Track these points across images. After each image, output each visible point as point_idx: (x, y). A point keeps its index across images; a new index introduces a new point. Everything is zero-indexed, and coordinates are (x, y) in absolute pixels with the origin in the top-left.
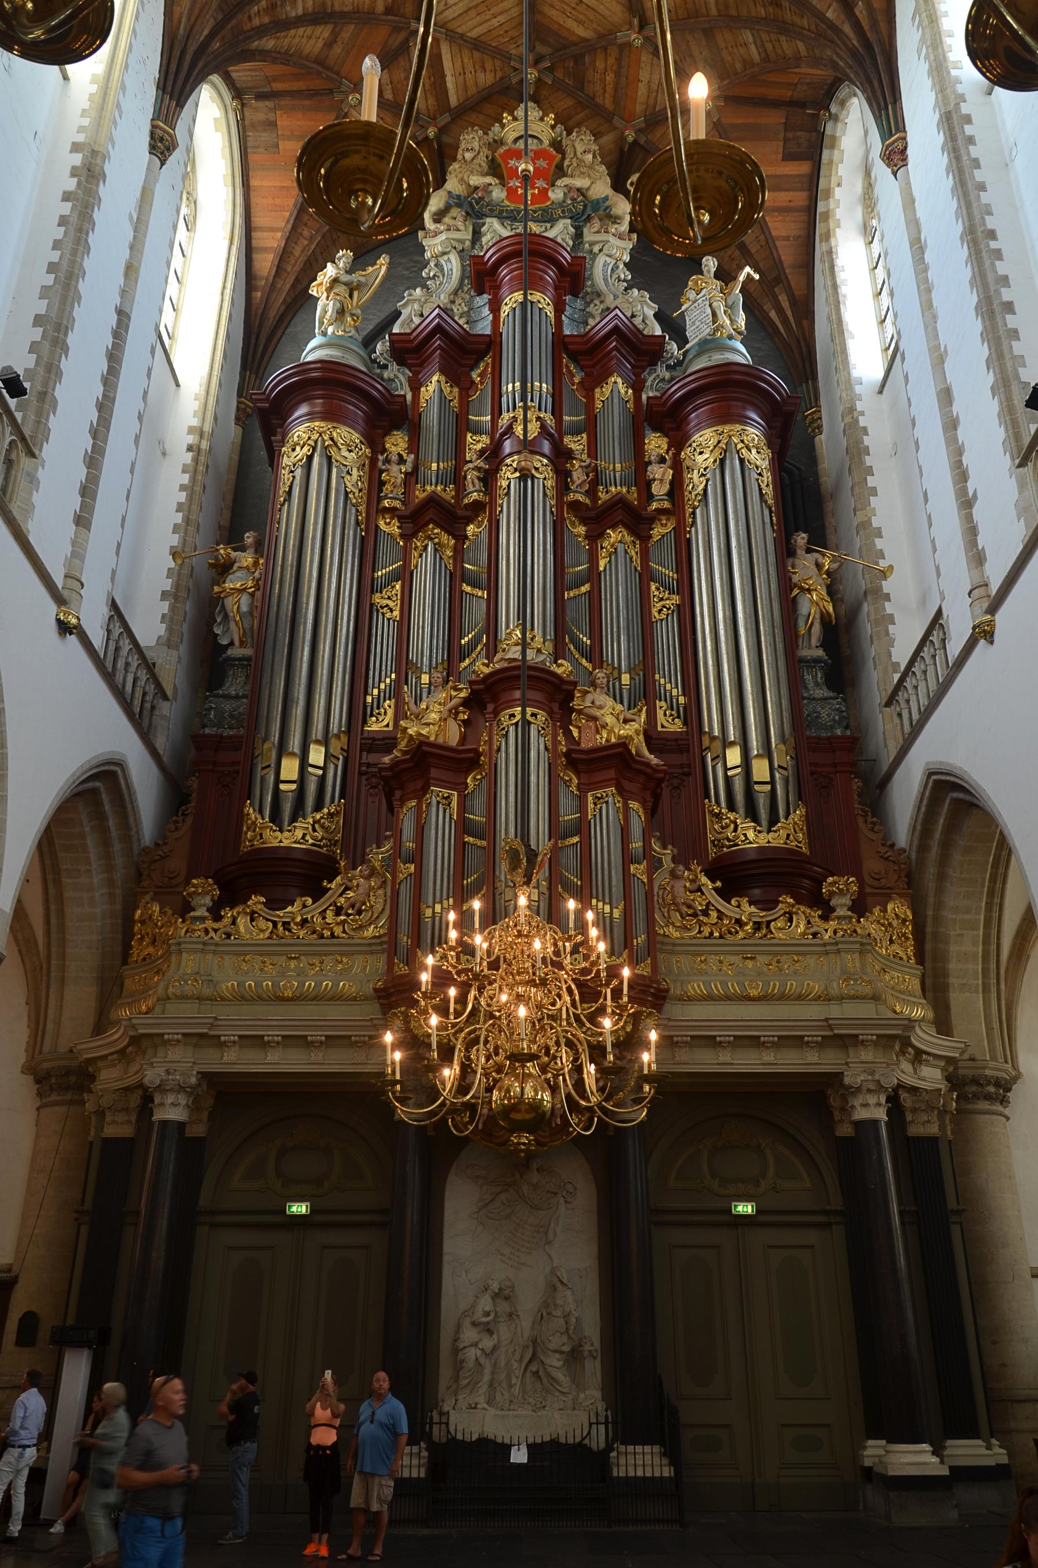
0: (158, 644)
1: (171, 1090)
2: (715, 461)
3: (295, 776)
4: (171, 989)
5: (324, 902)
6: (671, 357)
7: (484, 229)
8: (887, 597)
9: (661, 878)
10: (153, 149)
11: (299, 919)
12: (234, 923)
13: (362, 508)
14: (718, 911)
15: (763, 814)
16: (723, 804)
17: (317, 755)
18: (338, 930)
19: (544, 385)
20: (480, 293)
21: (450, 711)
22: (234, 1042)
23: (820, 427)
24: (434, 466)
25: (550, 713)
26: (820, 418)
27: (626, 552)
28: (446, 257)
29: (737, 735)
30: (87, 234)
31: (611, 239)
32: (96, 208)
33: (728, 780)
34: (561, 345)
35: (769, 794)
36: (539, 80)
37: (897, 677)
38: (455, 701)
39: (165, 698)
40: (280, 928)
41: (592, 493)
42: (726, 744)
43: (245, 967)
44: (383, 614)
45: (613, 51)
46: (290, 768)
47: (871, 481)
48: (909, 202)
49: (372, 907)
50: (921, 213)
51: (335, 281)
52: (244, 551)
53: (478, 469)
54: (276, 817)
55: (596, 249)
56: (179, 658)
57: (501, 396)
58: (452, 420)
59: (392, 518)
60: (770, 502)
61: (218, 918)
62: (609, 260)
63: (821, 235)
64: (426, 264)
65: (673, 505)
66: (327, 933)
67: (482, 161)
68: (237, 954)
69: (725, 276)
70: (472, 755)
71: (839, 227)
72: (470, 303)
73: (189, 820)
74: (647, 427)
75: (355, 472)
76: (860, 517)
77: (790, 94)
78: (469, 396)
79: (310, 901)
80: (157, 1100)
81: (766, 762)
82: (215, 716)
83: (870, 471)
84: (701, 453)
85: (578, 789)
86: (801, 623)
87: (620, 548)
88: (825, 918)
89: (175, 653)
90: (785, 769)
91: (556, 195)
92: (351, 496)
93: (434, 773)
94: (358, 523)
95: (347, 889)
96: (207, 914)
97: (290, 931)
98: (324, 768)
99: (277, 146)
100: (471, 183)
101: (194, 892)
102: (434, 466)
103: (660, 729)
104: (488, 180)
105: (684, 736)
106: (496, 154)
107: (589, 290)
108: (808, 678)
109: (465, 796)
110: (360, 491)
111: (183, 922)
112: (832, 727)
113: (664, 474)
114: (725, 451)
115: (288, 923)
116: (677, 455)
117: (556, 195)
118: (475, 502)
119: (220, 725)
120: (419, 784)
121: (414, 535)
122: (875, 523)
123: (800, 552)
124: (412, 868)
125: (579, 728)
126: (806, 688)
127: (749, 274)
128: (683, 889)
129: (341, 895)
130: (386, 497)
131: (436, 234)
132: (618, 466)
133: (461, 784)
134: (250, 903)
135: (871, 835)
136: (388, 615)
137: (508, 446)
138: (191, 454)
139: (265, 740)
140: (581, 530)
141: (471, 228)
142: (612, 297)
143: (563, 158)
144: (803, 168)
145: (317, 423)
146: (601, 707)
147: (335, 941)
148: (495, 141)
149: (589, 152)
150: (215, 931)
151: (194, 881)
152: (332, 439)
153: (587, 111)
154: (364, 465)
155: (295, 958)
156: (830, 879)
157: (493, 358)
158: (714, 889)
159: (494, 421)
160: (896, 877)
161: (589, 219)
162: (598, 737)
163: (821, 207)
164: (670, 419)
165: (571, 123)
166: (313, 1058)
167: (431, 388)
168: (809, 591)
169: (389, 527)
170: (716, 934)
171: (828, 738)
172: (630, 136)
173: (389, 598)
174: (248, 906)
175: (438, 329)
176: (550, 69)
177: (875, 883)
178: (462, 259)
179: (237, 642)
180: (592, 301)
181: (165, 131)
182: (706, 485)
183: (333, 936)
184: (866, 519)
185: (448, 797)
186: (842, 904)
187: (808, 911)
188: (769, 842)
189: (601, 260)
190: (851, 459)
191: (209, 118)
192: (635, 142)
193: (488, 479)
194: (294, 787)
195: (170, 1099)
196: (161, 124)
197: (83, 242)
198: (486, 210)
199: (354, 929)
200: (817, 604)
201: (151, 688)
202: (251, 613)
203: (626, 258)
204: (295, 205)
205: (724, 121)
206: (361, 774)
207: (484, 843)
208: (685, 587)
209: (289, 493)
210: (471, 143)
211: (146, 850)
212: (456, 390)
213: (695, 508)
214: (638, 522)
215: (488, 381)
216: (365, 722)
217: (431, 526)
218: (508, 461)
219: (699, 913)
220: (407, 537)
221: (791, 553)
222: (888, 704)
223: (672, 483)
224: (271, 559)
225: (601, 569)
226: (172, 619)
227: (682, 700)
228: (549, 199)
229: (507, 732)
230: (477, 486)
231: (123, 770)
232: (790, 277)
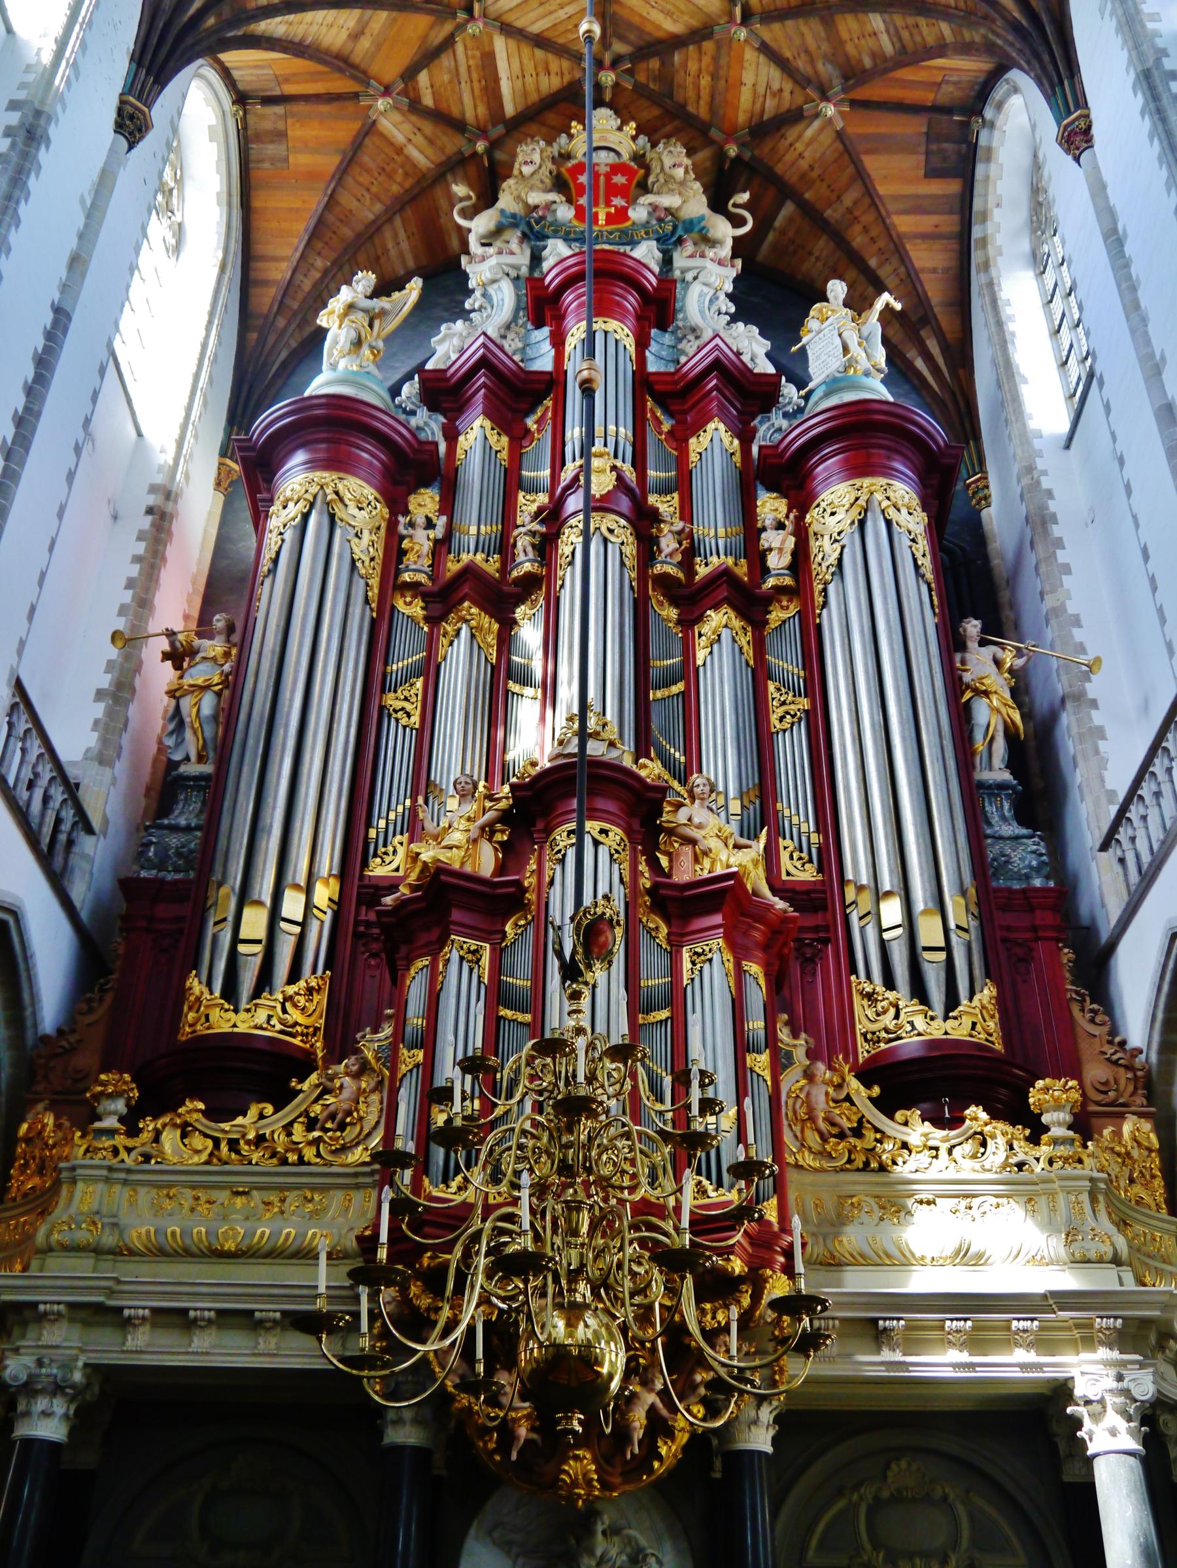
0: (85, 758)
1: (42, 1392)
2: (853, 523)
3: (261, 933)
4: (56, 1236)
5: (291, 1111)
7: (545, 253)
8: (1094, 704)
9: (792, 1080)
10: (119, 127)
11: (251, 1136)
12: (157, 1139)
13: (375, 582)
14: (877, 1130)
15: (937, 994)
17: (293, 906)
18: (309, 1153)
19: (622, 430)
20: (538, 325)
21: (482, 829)
22: (144, 1318)
23: (986, 498)
24: (473, 530)
25: (628, 831)
26: (987, 487)
27: (734, 641)
28: (495, 286)
29: (896, 881)
30: (18, 203)
31: (710, 265)
32: (33, 175)
33: (883, 946)
35: (943, 965)
36: (616, 85)
37: (1113, 810)
38: (489, 815)
39: (90, 831)
41: (687, 563)
42: (879, 896)
43: (168, 1205)
44: (397, 720)
45: (708, 46)
46: (254, 923)
47: (1062, 556)
48: (1098, 189)
49: (361, 1119)
50: (1115, 197)
51: (351, 307)
52: (211, 638)
53: (533, 533)
54: (230, 992)
55: (689, 276)
56: (114, 782)
57: (564, 445)
58: (499, 475)
59: (414, 597)
60: (930, 576)
62: (706, 289)
63: (978, 265)
64: (473, 291)
65: (797, 580)
66: (292, 1157)
68: (158, 1186)
69: (857, 304)
70: (512, 890)
71: (1001, 254)
73: (109, 998)
74: (760, 487)
75: (366, 535)
76: (1050, 601)
77: (931, 96)
78: (522, 447)
79: (269, 1109)
80: (21, 1407)
81: (938, 920)
82: (155, 854)
83: (1059, 543)
84: (833, 514)
85: (669, 942)
86: (979, 736)
87: (726, 635)
88: (1034, 1140)
89: (108, 771)
90: (966, 930)
91: (638, 214)
92: (359, 564)
93: (456, 915)
94: (367, 601)
95: (326, 1091)
96: (117, 1125)
97: (238, 1152)
98: (303, 925)
99: (286, 160)
101: (102, 1093)
103: (784, 877)
104: (553, 196)
105: (818, 887)
106: (563, 170)
107: (680, 324)
108: (991, 809)
109: (502, 950)
110: (372, 559)
111: (83, 1137)
112: (1027, 877)
113: (783, 542)
114: (866, 511)
115: (237, 1141)
116: (800, 519)
118: (528, 575)
119: (161, 867)
120: (434, 935)
121: (443, 617)
122: (1071, 608)
123: (973, 645)
124: (420, 1055)
125: (669, 855)
126: (990, 824)
127: (887, 305)
128: (822, 1098)
129: (316, 1101)
130: (407, 569)
133: (497, 932)
135: (1092, 1029)
136: (404, 721)
138: (150, 518)
139: (220, 884)
140: (672, 613)
141: (528, 252)
143: (647, 175)
144: (952, 187)
145: (318, 474)
146: (700, 827)
147: (303, 1169)
148: (560, 155)
149: (680, 165)
150: (129, 1150)
151: (103, 1077)
152: (337, 493)
153: (677, 123)
154: (378, 528)
155: (243, 1193)
156: (1040, 1084)
158: (870, 1098)
159: (555, 477)
160: (1131, 1088)
161: (680, 241)
162: (698, 867)
163: (976, 232)
164: (787, 474)
165: (657, 136)
166: (262, 1347)
167: (472, 436)
168: (986, 693)
169: (411, 608)
170: (874, 1165)
171: (1024, 891)
172: (732, 151)
173: (406, 699)
174: (179, 1116)
175: (484, 363)
176: (630, 72)
177: (1100, 1097)
178: (516, 287)
179: (193, 757)
180: (685, 336)
181: (136, 108)
182: (841, 554)
183: (301, 1161)
184: (1057, 604)
185: (476, 951)
186: (1057, 1121)
187: (1009, 1129)
188: (946, 1033)
189: (695, 290)
190: (1033, 530)
191: (197, 107)
192: (738, 157)
193: (546, 547)
194: (258, 948)
195: (41, 1404)
196: (131, 99)
197: (10, 212)
199: (333, 1152)
200: (998, 711)
201: (68, 814)
202: (215, 718)
203: (729, 287)
204: (306, 230)
205: (849, 130)
206: (356, 935)
207: (528, 1018)
209: (275, 561)
210: (531, 157)
211: (45, 1039)
212: (505, 440)
213: (826, 583)
214: (751, 604)
215: (549, 428)
216: (365, 864)
217: (466, 604)
219: (848, 1133)
220: (434, 620)
222: (1104, 847)
223: (794, 554)
224: (244, 646)
225: (699, 662)
226: (107, 728)
227: (814, 838)
228: (627, 218)
229: (564, 856)
231: (17, 921)
232: (940, 317)
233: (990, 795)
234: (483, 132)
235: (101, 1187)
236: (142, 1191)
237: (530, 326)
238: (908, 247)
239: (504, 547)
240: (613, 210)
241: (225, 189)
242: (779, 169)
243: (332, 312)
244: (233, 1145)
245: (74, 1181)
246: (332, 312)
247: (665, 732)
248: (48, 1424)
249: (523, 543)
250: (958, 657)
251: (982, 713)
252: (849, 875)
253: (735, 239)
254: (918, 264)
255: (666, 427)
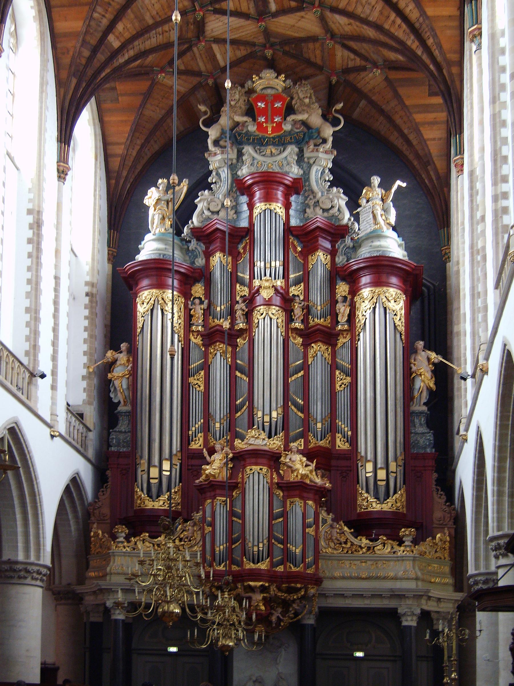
6: (354, 233)
11: (164, 543)
12: (136, 543)
16: (365, 488)
20: (243, 194)
24: (218, 309)
28: (222, 169)
31: (321, 155)
34: (288, 230)
40: (156, 547)
49: (195, 538)
53: (244, 311)
55: (311, 161)
61: (129, 542)
62: (319, 168)
64: (211, 172)
65: (350, 326)
67: (241, 103)
72: (236, 200)
74: (338, 278)
80: (112, 611)
87: (319, 354)
96: (124, 540)
99: (118, 99)
100: (235, 119)
102: (218, 309)
104: (245, 119)
106: (250, 99)
107: (307, 188)
108: (417, 421)
112: (425, 448)
113: (344, 310)
115: (159, 544)
117: (287, 127)
118: (241, 329)
131: (215, 154)
132: (319, 308)
134: (142, 536)
135: (440, 501)
137: (259, 300)
140: (300, 340)
141: (236, 151)
142: (320, 194)
143: (292, 98)
145: (154, 291)
149: (307, 97)
152: (163, 299)
157: (250, 239)
161: (307, 143)
171: (422, 454)
172: (334, 80)
180: (309, 196)
189: (314, 169)
192: (337, 82)
193: (248, 316)
198: (244, 140)
203: (330, 165)
208: (353, 373)
212: (230, 259)
218: (258, 308)
221: (415, 351)
223: (349, 315)
228: (282, 129)
230: (242, 319)
233: (417, 416)
234: (211, 75)
235: (123, 557)
236: (134, 558)
237: (238, 193)
238: (421, 129)
239: (232, 313)
240: (275, 125)
241: (91, 118)
242: (359, 85)
243: (150, 197)
244: (158, 545)
245: (114, 556)
246: (150, 197)
247: (295, 393)
248: (119, 615)
249: (239, 313)
250: (413, 357)
251: (419, 384)
252: (359, 451)
253: (335, 134)
254: (426, 137)
255: (299, 249)
